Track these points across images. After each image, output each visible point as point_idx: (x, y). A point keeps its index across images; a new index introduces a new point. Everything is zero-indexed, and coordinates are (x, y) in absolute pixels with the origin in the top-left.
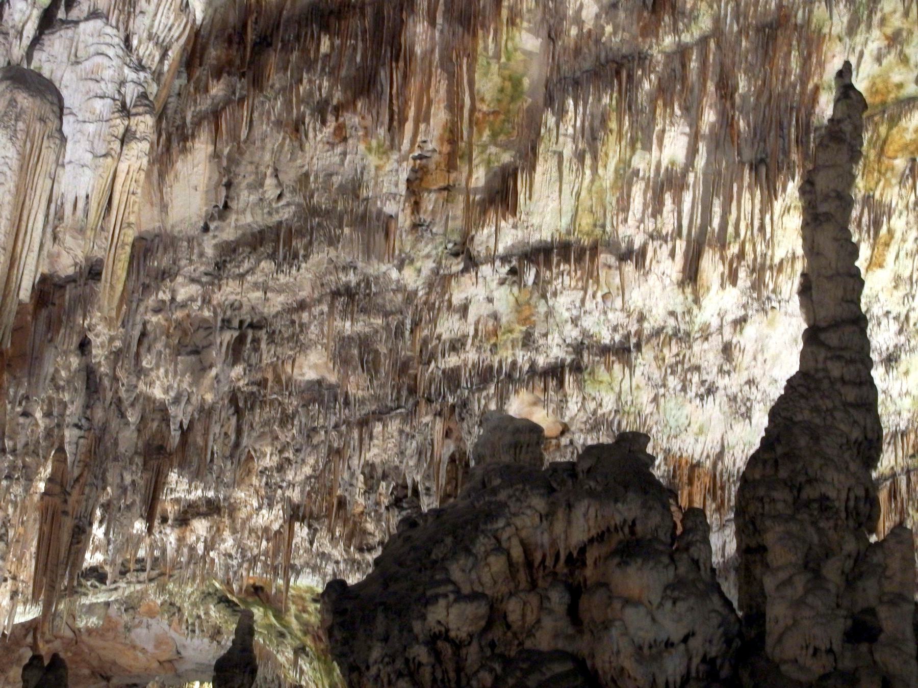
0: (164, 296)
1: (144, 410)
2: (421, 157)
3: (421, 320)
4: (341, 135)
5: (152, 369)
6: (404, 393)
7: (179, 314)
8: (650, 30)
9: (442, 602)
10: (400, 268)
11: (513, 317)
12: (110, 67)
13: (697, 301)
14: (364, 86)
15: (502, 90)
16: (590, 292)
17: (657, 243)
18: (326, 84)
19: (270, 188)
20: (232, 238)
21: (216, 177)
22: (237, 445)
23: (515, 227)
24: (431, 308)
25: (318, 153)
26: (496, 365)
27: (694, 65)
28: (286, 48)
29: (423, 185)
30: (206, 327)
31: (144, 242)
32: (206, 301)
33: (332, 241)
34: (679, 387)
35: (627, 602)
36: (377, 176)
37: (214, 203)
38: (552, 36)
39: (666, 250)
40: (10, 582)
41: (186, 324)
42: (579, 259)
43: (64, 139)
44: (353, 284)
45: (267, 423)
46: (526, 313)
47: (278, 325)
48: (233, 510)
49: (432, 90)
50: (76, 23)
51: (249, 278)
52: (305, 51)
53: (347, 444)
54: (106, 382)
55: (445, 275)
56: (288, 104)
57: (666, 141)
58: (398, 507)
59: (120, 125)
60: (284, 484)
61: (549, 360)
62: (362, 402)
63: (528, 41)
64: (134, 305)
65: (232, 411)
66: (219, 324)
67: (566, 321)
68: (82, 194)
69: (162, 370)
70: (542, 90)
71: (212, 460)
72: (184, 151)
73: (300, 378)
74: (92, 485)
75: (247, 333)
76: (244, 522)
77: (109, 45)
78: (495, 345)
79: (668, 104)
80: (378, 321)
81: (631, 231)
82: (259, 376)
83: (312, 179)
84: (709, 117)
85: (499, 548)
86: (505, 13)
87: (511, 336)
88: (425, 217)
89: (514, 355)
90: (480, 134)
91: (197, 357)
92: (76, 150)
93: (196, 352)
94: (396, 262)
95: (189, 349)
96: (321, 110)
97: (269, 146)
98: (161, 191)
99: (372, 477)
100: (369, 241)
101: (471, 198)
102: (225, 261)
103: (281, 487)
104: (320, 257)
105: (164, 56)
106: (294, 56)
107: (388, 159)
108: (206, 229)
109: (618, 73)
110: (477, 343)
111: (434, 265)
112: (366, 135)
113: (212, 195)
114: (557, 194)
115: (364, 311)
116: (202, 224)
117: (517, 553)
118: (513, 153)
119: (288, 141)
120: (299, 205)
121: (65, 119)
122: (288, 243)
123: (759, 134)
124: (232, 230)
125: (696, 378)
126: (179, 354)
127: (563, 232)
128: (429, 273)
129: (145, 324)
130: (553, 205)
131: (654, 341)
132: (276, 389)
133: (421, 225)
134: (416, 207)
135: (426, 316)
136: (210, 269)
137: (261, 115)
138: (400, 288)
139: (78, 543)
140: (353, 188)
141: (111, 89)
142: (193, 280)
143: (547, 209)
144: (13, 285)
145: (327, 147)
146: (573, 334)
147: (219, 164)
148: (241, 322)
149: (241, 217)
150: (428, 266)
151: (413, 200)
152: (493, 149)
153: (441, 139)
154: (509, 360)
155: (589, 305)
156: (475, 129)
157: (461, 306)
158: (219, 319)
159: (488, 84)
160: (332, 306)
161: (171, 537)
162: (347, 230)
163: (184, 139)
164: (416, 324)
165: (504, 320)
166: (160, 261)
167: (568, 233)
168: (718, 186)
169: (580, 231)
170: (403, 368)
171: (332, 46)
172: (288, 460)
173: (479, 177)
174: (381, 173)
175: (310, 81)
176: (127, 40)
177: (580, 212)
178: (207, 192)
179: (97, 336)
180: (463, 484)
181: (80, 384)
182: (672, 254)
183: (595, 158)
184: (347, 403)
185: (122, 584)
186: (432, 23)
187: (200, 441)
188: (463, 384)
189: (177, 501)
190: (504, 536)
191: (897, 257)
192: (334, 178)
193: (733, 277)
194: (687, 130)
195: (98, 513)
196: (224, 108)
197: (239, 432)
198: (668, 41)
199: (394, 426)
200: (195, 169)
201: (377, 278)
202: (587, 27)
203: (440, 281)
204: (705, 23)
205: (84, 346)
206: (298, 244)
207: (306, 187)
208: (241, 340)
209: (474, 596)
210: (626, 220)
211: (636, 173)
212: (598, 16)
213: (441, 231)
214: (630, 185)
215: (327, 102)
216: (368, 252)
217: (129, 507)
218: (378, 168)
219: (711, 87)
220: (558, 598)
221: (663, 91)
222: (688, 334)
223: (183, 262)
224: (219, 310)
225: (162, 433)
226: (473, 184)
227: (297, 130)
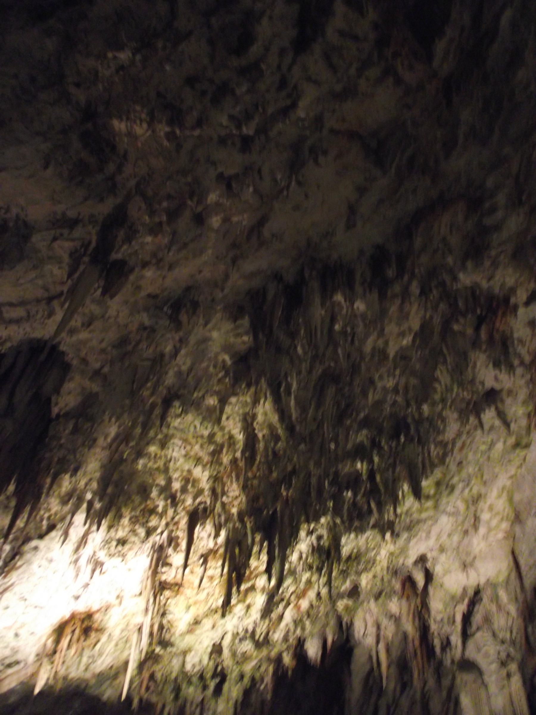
50: (473, 635)
176: (494, 635)
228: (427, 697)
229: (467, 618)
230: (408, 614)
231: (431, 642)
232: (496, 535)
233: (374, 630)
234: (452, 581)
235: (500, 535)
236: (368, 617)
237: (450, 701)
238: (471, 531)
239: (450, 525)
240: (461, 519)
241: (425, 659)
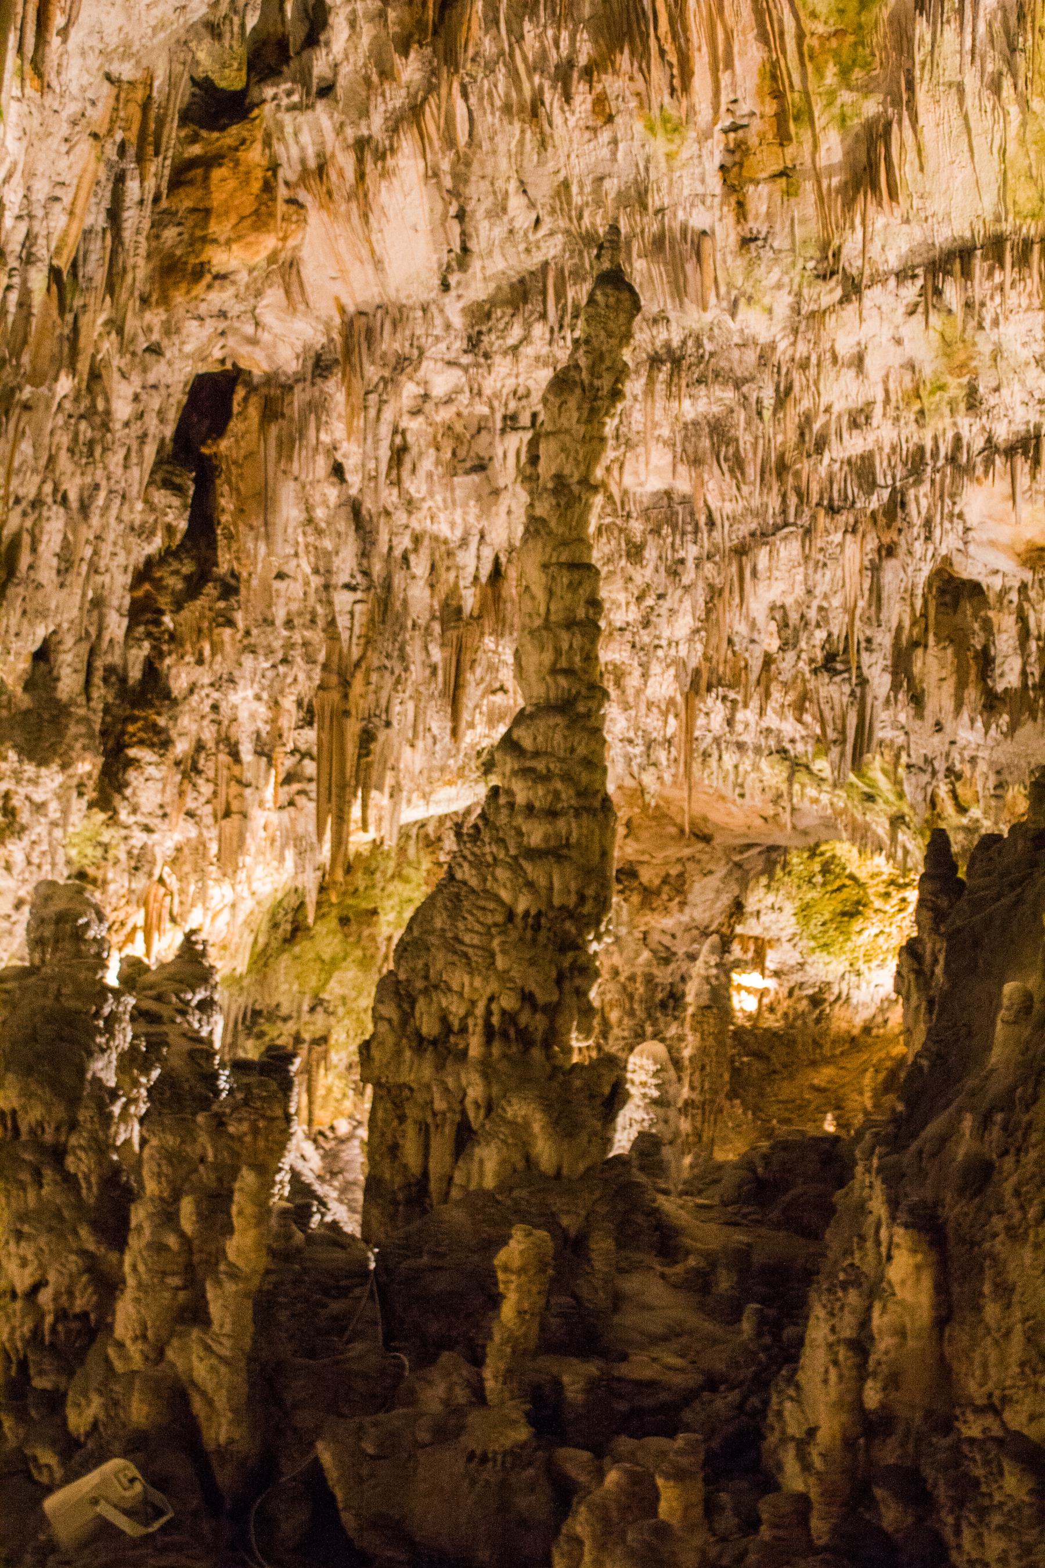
1: (432, 554)
2: (735, 128)
3: (789, 389)
4: (603, 112)
5: (423, 499)
6: (793, 500)
7: (445, 414)
11: (940, 364)
20: (482, 296)
21: (439, 206)
23: (907, 221)
25: (576, 146)
26: (929, 445)
29: (745, 173)
31: (363, 319)
36: (671, 169)
37: (446, 248)
41: (459, 428)
42: (1023, 260)
44: (675, 344)
46: (962, 356)
49: (727, 11)
51: (528, 351)
55: (812, 314)
56: (514, 75)
58: (828, 670)
60: (664, 643)
61: (1014, 428)
62: (733, 520)
64: (372, 413)
66: (499, 425)
67: (1027, 364)
69: (439, 498)
73: (639, 490)
76: (639, 692)
78: (922, 412)
80: (729, 395)
83: (574, 189)
87: (946, 396)
88: (756, 225)
89: (955, 424)
90: (820, 72)
91: (482, 475)
93: (481, 467)
94: (725, 304)
95: (468, 464)
97: (502, 148)
98: (369, 241)
99: (787, 625)
100: (676, 280)
101: (825, 184)
102: (480, 333)
107: (683, 139)
108: (446, 287)
110: (891, 411)
111: (791, 299)
112: (641, 106)
113: (441, 237)
114: (968, 155)
116: (436, 282)
118: (880, 97)
119: (528, 135)
124: (480, 285)
126: (455, 475)
127: (990, 218)
128: (788, 312)
130: (962, 175)
132: (608, 510)
133: (756, 239)
137: (481, 99)
139: (368, 755)
145: (587, 135)
147: (439, 185)
149: (487, 262)
150: (783, 302)
151: (733, 200)
152: (846, 96)
153: (760, 94)
154: (950, 435)
156: (810, 67)
157: (853, 356)
158: (498, 416)
160: (651, 381)
163: (381, 156)
164: (783, 396)
165: (927, 371)
166: (390, 344)
167: (998, 220)
169: (1017, 214)
173: (832, 148)
174: (677, 163)
175: (539, 37)
177: (1011, 181)
178: (432, 231)
180: (938, 624)
181: (344, 525)
184: (711, 523)
188: (880, 481)
192: (607, 184)
196: (425, 99)
199: (789, 549)
205: (338, 471)
207: (569, 204)
213: (786, 245)
215: (570, 63)
218: (669, 156)
224: (496, 403)
226: (823, 161)
227: (535, 114)
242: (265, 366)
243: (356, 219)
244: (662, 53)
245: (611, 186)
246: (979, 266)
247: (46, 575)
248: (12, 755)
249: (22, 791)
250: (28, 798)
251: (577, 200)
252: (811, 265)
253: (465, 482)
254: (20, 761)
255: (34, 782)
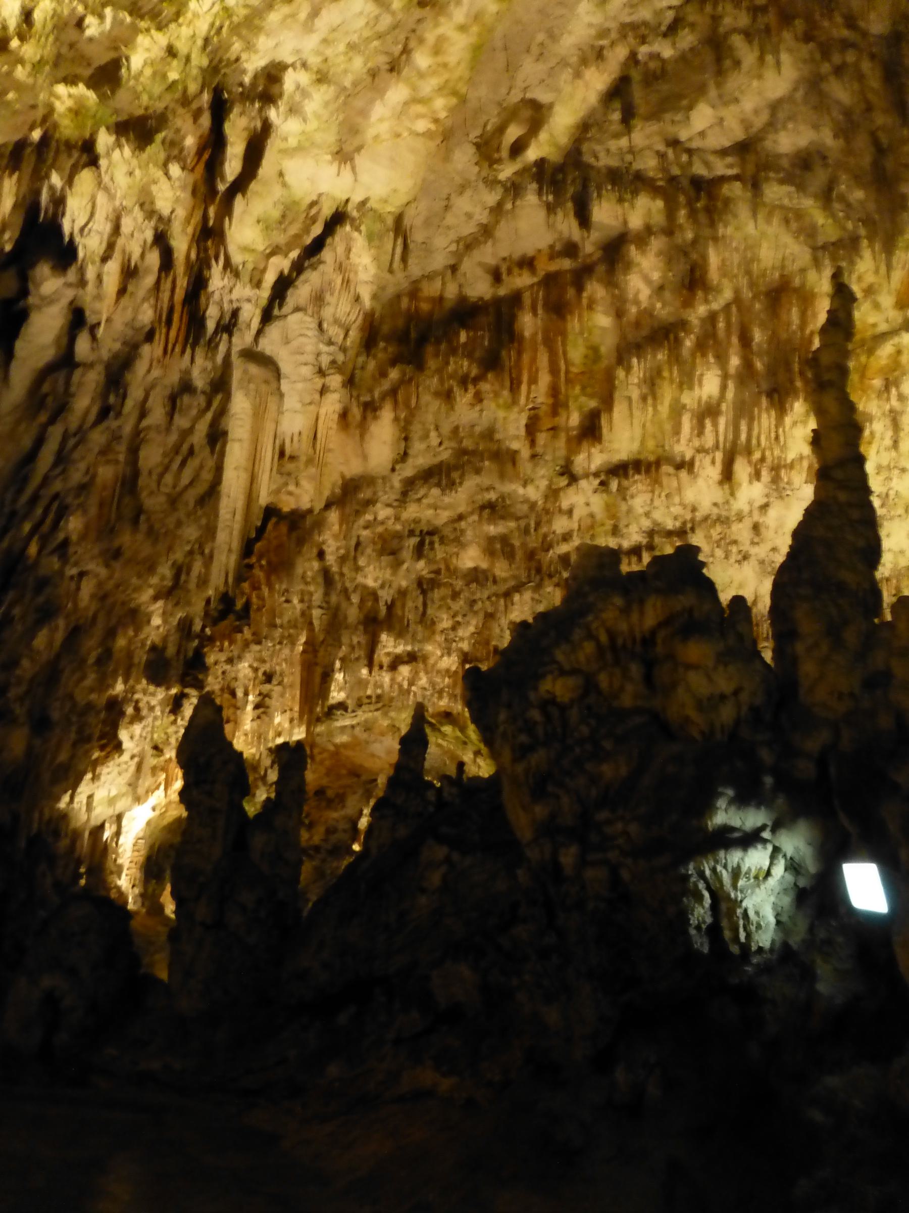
0: (369, 517)
2: (533, 409)
4: (479, 398)
6: (533, 572)
7: (380, 529)
8: (688, 303)
9: (549, 678)
10: (525, 485)
12: (310, 343)
13: (732, 494)
14: (491, 363)
15: (586, 357)
16: (657, 493)
17: (702, 455)
18: (466, 363)
19: (434, 439)
22: (424, 613)
23: (601, 452)
24: (547, 511)
25: (465, 412)
27: (721, 325)
28: (438, 342)
30: (398, 536)
32: (397, 518)
33: (478, 471)
34: (723, 556)
35: (689, 667)
38: (619, 314)
39: (708, 459)
40: (288, 712)
42: (648, 471)
43: (282, 395)
45: (443, 599)
47: (447, 531)
48: (425, 658)
50: (286, 316)
51: (425, 501)
52: (450, 342)
53: (496, 610)
54: (337, 577)
56: (442, 381)
57: (705, 382)
59: (319, 382)
60: (457, 639)
62: (505, 580)
63: (603, 320)
65: (419, 592)
66: (406, 533)
67: (641, 515)
68: (296, 431)
70: (615, 354)
71: (408, 625)
72: (376, 418)
74: (331, 645)
75: (426, 539)
77: (308, 328)
79: (704, 355)
80: (512, 524)
81: (683, 448)
82: (435, 567)
83: (461, 429)
84: (735, 361)
85: (591, 636)
86: (585, 302)
88: (539, 449)
90: (573, 388)
92: (291, 402)
93: (393, 553)
96: (464, 381)
103: (455, 641)
104: (471, 483)
105: (346, 335)
106: (443, 346)
109: (667, 337)
115: (503, 518)
117: (604, 638)
120: (452, 449)
121: (282, 381)
122: (448, 475)
123: (771, 371)
125: (734, 549)
129: (358, 537)
130: (627, 434)
131: (704, 525)
134: (533, 443)
135: (544, 519)
136: (398, 497)
138: (526, 501)
140: (489, 434)
141: (310, 358)
142: (389, 505)
143: (623, 438)
144: (254, 495)
146: (646, 524)
148: (421, 531)
150: (543, 484)
152: (583, 399)
155: (657, 502)
159: (576, 353)
160: (480, 516)
161: (386, 678)
162: (487, 463)
164: (538, 525)
167: (639, 453)
168: (744, 411)
170: (531, 555)
171: (468, 337)
172: (458, 623)
173: (575, 419)
175: (456, 363)
176: (320, 325)
179: (329, 547)
181: (320, 580)
182: (713, 462)
183: (655, 398)
185: (360, 713)
186: (535, 314)
187: (400, 613)
189: (388, 654)
190: (594, 626)
191: (878, 452)
193: (757, 475)
194: (719, 372)
195: (338, 664)
197: (425, 605)
198: (702, 310)
199: (528, 595)
200: (383, 432)
201: (509, 494)
202: (643, 306)
203: (553, 494)
204: (728, 294)
205: (321, 555)
206: (455, 475)
208: (421, 544)
209: (574, 672)
210: (678, 441)
211: (684, 407)
212: (650, 297)
214: (680, 415)
216: (502, 476)
217: (357, 659)
219: (735, 340)
220: (635, 669)
221: (701, 347)
222: (728, 518)
223: (380, 494)
225: (376, 611)
228: (142, 435)
229: (283, 286)
230: (188, 221)
231: (203, 307)
232: (419, 116)
233: (108, 228)
234: (303, 170)
235: (422, 125)
236: (101, 198)
237: (177, 453)
238: (384, 75)
239: (361, 22)
240: (386, 21)
241: (181, 339)
242: (293, 506)
243: (358, 437)
244: (511, 374)
245: (478, 429)
246: (631, 472)
247: (192, 585)
248: (144, 681)
249: (145, 699)
250: (148, 703)
251: (462, 434)
252: (558, 468)
253: (385, 559)
254: (148, 684)
255: (153, 694)
